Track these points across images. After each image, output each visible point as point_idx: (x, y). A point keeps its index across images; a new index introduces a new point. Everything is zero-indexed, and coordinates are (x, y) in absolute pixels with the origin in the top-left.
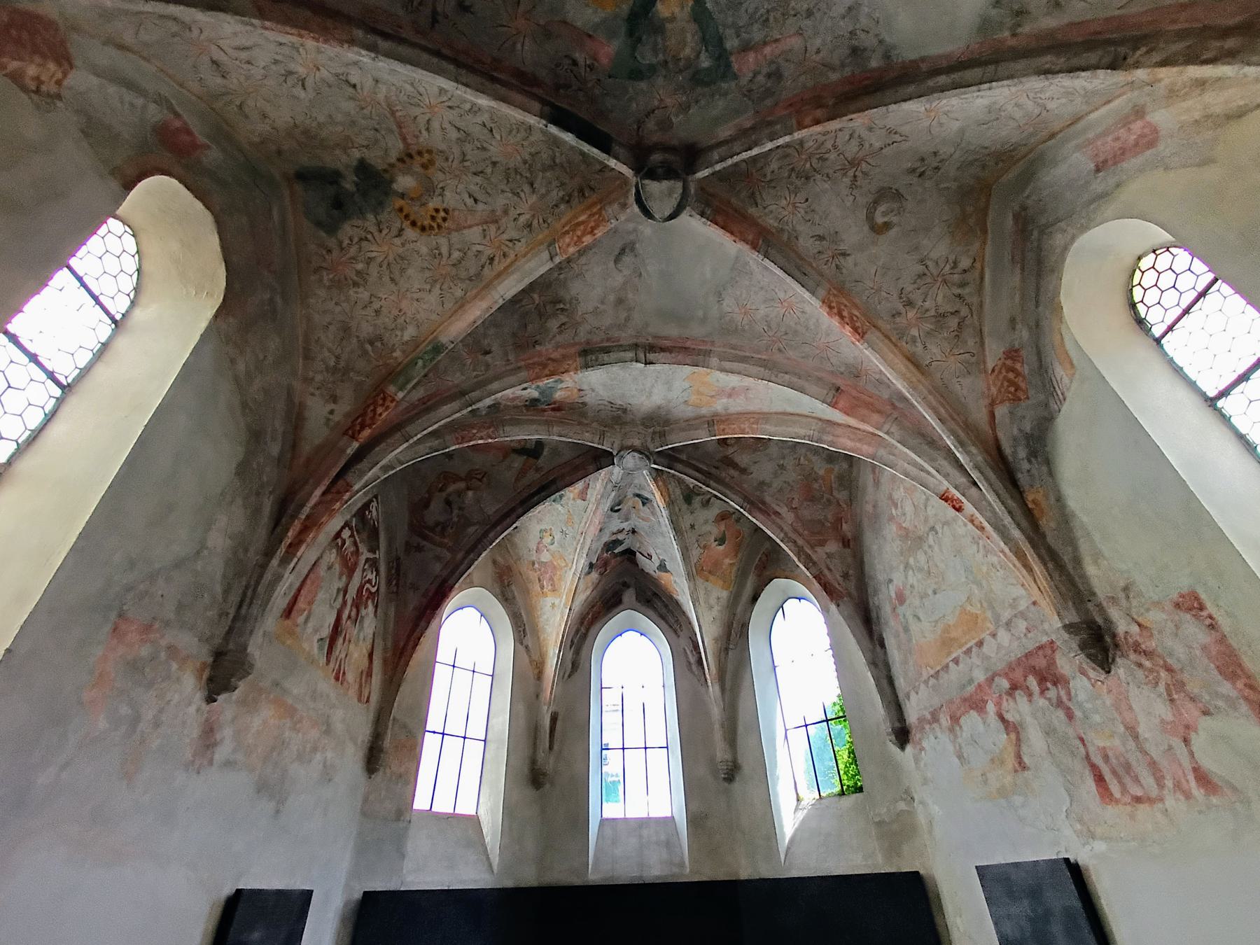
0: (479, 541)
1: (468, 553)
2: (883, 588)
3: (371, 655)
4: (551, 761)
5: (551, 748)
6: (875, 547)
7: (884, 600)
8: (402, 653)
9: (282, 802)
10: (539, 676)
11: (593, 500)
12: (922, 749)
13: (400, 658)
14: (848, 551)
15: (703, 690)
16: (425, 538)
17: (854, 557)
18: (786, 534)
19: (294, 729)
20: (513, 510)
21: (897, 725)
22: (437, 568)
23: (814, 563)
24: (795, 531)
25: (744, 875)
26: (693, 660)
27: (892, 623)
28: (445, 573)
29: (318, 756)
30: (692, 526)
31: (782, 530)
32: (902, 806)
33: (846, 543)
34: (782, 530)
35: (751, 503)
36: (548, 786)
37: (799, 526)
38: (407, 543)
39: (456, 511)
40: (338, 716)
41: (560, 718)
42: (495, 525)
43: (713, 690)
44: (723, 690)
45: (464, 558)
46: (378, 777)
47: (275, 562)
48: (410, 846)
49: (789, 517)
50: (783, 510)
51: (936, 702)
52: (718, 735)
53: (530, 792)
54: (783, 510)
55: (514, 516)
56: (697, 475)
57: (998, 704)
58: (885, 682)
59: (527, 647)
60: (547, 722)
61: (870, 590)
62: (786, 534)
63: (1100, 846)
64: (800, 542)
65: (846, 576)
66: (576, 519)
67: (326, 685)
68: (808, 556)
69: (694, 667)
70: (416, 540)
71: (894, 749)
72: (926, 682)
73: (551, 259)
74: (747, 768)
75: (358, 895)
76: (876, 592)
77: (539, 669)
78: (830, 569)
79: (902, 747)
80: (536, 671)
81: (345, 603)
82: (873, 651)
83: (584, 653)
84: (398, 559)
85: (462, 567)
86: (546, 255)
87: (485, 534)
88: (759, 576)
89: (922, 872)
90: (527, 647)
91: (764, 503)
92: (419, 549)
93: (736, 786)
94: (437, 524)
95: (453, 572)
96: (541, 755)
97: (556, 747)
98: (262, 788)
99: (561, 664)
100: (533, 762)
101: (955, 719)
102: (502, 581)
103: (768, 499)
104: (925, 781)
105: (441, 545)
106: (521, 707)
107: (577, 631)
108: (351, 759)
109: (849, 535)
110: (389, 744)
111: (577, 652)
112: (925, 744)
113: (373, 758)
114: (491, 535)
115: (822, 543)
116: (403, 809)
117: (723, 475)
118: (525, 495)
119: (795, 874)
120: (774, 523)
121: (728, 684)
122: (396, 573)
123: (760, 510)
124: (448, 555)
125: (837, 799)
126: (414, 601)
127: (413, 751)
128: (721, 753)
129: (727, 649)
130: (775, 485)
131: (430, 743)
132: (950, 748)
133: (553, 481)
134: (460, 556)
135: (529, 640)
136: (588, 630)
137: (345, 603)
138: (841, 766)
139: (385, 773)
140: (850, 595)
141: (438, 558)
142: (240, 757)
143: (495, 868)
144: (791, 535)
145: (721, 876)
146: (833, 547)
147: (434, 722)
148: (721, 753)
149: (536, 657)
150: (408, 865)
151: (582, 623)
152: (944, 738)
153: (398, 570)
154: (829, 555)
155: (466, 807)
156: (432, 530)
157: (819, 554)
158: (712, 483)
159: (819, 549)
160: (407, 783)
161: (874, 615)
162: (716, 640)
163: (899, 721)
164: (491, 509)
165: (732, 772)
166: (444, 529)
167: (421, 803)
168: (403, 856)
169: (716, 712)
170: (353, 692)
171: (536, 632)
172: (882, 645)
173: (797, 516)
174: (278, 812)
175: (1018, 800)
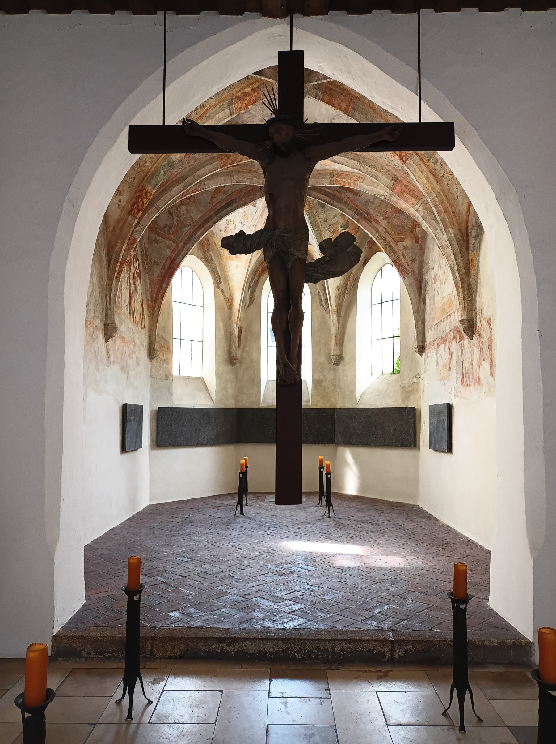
0: (191, 236)
1: (186, 243)
2: (430, 271)
3: (142, 305)
4: (240, 351)
5: (239, 346)
7: (429, 277)
8: (155, 301)
9: (128, 374)
10: (230, 307)
11: (260, 207)
13: (155, 304)
14: (417, 245)
15: (328, 315)
16: (159, 235)
17: (421, 249)
18: (380, 234)
19: (126, 346)
20: (210, 218)
21: (421, 344)
22: (168, 252)
23: (395, 253)
24: (387, 232)
25: (338, 407)
26: (323, 299)
27: (430, 292)
28: (173, 255)
29: (134, 356)
30: (325, 221)
31: (377, 231)
32: (415, 380)
33: (417, 240)
34: (377, 231)
35: (360, 214)
36: (238, 364)
37: (389, 229)
38: (149, 238)
39: (176, 218)
40: (137, 336)
41: (243, 330)
42: (200, 227)
43: (334, 317)
44: (339, 317)
45: (183, 247)
46: (155, 361)
47: (114, 283)
48: (174, 391)
49: (384, 222)
50: (380, 219)
51: (435, 336)
52: (333, 342)
53: (229, 368)
54: (380, 219)
55: (212, 222)
56: (325, 197)
57: (449, 343)
58: (420, 322)
59: (222, 290)
60: (236, 332)
61: (424, 271)
62: (380, 234)
63: (458, 399)
64: (388, 239)
65: (413, 260)
66: (249, 216)
67: (131, 325)
68: (392, 249)
69: (324, 303)
70: (154, 236)
72: (435, 326)
73: (231, 115)
74: (346, 359)
75: (156, 408)
76: (427, 272)
77: (230, 302)
78: (404, 256)
79: (421, 355)
80: (229, 304)
81: (130, 284)
82: (419, 306)
83: (257, 293)
84: (146, 248)
85: (183, 253)
86: (227, 111)
87: (195, 232)
88: (370, 248)
89: (416, 407)
90: (222, 290)
91: (368, 213)
92: (156, 241)
93: (341, 367)
94: (166, 226)
95: (177, 255)
96: (234, 350)
97: (242, 346)
98: (122, 369)
99: (243, 301)
100: (230, 352)
101: (438, 346)
102: (203, 249)
103: (371, 211)
104: (426, 371)
105: (169, 239)
106: (221, 325)
107: (253, 279)
108: (143, 354)
110: (157, 347)
111: (253, 292)
112: (429, 354)
113: (151, 353)
114: (199, 233)
115: (402, 240)
116: (168, 376)
117: (343, 196)
118: (218, 207)
119: (362, 406)
120: (373, 227)
121: (342, 314)
122: (146, 258)
123: (365, 218)
124: (174, 245)
125: (390, 375)
126: (157, 271)
127: (168, 348)
128: (334, 351)
129: (344, 293)
130: (376, 203)
131: (175, 344)
132: (435, 356)
133: (234, 200)
134: (181, 245)
135: (222, 286)
136: (259, 278)
137: (130, 284)
138: (396, 360)
139: (157, 359)
140: (413, 272)
141: (168, 247)
142: (116, 360)
143: (214, 400)
144: (383, 234)
145: (327, 406)
146: (408, 242)
147: (175, 334)
148: (334, 351)
149: (227, 296)
150: (174, 397)
151: (255, 274)
152: (434, 353)
153: (146, 255)
154: (406, 248)
155: (197, 374)
156: (163, 230)
157: (399, 247)
158: (335, 203)
159: (399, 244)
160: (168, 363)
161: (423, 285)
162: (338, 288)
163: (422, 342)
164: (196, 216)
165: (339, 360)
166: (169, 230)
167: (175, 372)
168: (172, 394)
169: (333, 330)
170: (139, 326)
171: (227, 281)
172: (424, 302)
173: (389, 223)
174: (128, 378)
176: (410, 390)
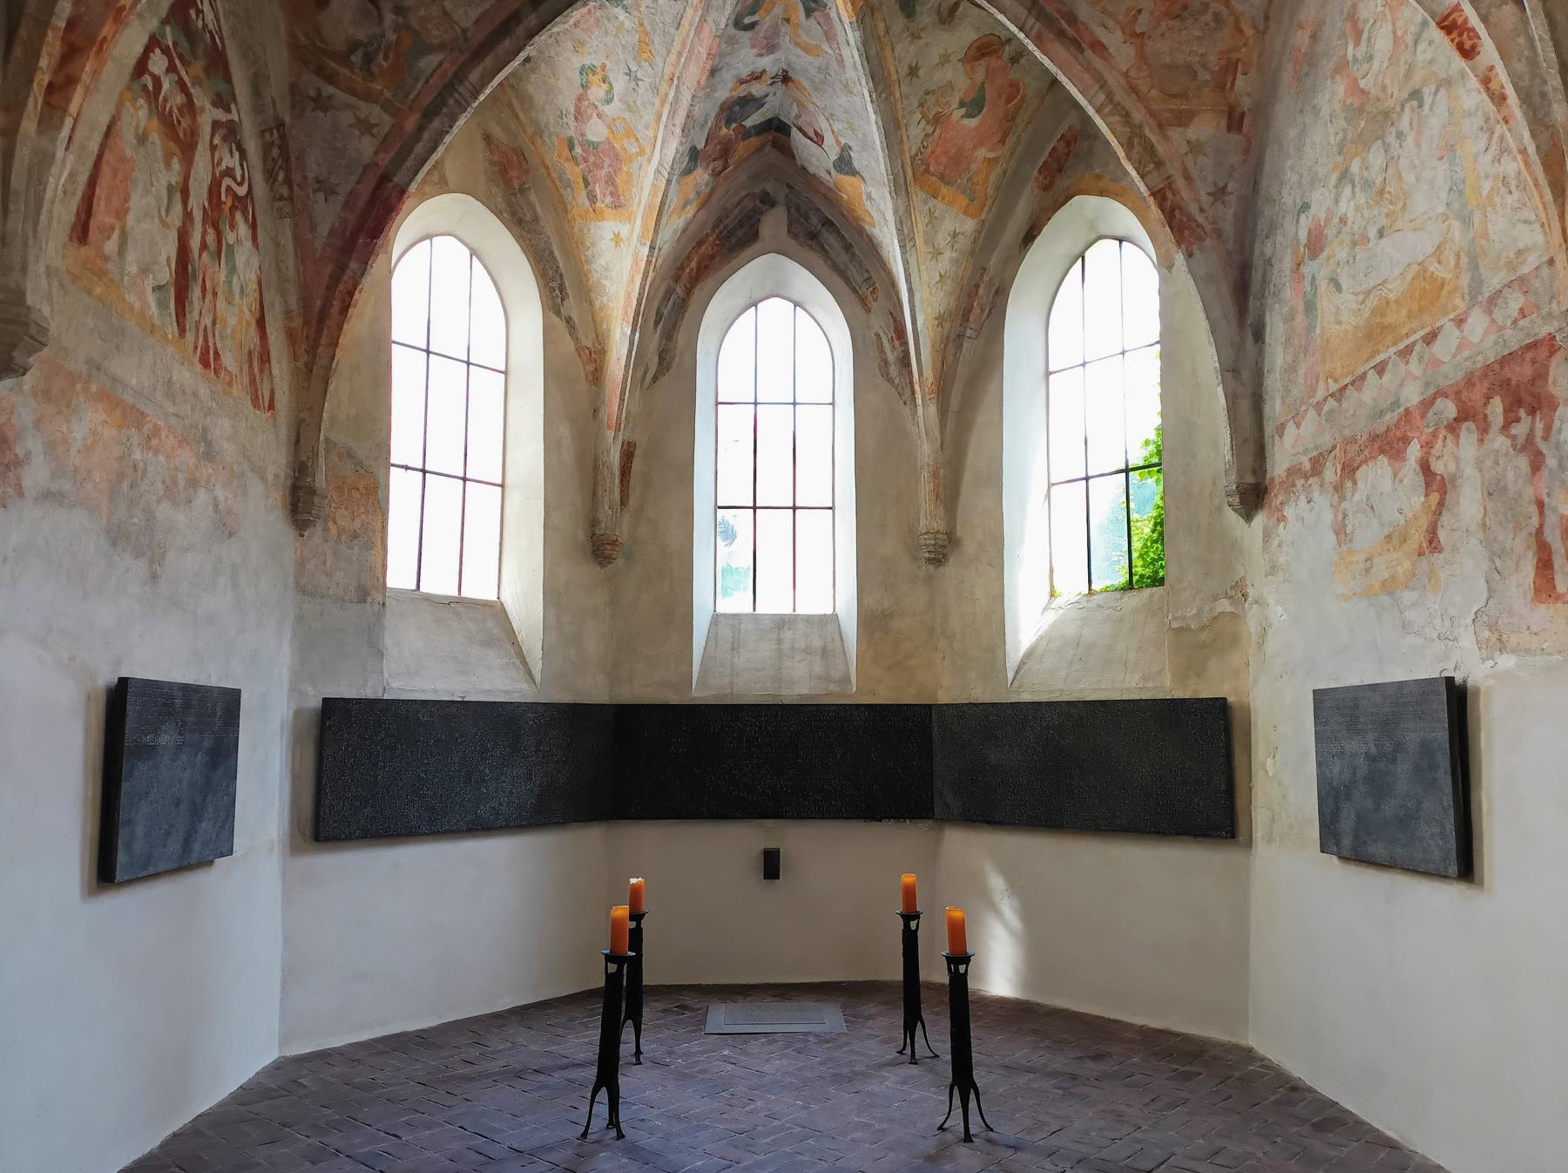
0: (450, 87)
1: (429, 114)
2: (1288, 224)
3: (261, 323)
4: (626, 521)
5: (624, 500)
6: (1292, 133)
7: (1282, 248)
8: (321, 321)
10: (596, 376)
12: (1284, 518)
13: (319, 332)
14: (1236, 138)
15: (907, 410)
16: (331, 79)
17: (1247, 151)
18: (1110, 96)
20: (516, 17)
21: (1250, 479)
22: (366, 147)
23: (1159, 164)
24: (1133, 89)
25: (943, 698)
26: (891, 356)
27: (1288, 293)
28: (385, 159)
29: (202, 497)
30: (913, 71)
31: (1103, 85)
32: (1224, 605)
33: (1235, 121)
34: (1103, 85)
36: (620, 562)
38: (293, 89)
39: (389, 18)
40: (221, 428)
41: (637, 452)
43: (926, 411)
44: (943, 412)
45: (421, 128)
46: (316, 535)
47: (29, 125)
48: (388, 641)
49: (1123, 53)
50: (1113, 39)
51: (1327, 440)
52: (925, 489)
53: (588, 572)
54: (1113, 39)
55: (520, 31)
57: (1428, 445)
58: (1245, 405)
59: (569, 320)
60: (615, 458)
61: (1262, 226)
62: (1110, 96)
63: (1507, 662)
64: (1138, 115)
65: (1219, 193)
67: (188, 375)
68: (1151, 150)
69: (893, 371)
70: (311, 83)
71: (1232, 518)
74: (969, 547)
75: (315, 703)
76: (1273, 227)
77: (595, 358)
78: (1188, 178)
79: (1248, 517)
80: (591, 368)
81: (188, 215)
82: (1239, 348)
83: (681, 338)
84: (280, 125)
85: (419, 148)
87: (461, 74)
88: (1046, 188)
89: (1231, 699)
90: (569, 320)
91: (1072, 19)
92: (322, 103)
93: (949, 570)
94: (354, 45)
95: (400, 159)
96: (605, 513)
97: (633, 501)
98: (117, 536)
99: (638, 358)
100: (594, 523)
101: (1349, 470)
102: (508, 182)
104: (1273, 570)
105: (367, 96)
106: (564, 431)
109: (1246, 103)
110: (329, 480)
111: (669, 336)
112: (1289, 512)
113: (301, 503)
114: (474, 76)
115: (1183, 119)
116: (368, 587)
119: (1026, 697)
120: (1088, 68)
121: (954, 404)
122: (281, 158)
123: (1061, 34)
124: (387, 121)
125: (1118, 595)
126: (327, 216)
127: (370, 495)
128: (928, 519)
129: (960, 336)
132: (1328, 516)
134: (411, 123)
135: (571, 307)
136: (689, 292)
137: (188, 215)
138: (1136, 545)
139: (326, 529)
140: (1218, 234)
141: (366, 127)
142: (67, 486)
143: (538, 677)
145: (909, 697)
146: (1206, 128)
147: (403, 446)
148: (928, 519)
149: (587, 342)
150: (389, 666)
151: (677, 279)
152: (1323, 501)
153: (284, 149)
154: (1195, 148)
155: (479, 588)
156: (344, 59)
159: (1174, 133)
160: (369, 546)
161: (1257, 276)
162: (940, 319)
163: (1254, 472)
165: (943, 549)
166: (369, 59)
167: (399, 576)
168: (380, 654)
169: (926, 451)
170: (239, 391)
171: (586, 293)
172: (1259, 336)
173: (1141, 55)
174: (154, 576)
175: (1408, 596)
176: (1213, 637)
